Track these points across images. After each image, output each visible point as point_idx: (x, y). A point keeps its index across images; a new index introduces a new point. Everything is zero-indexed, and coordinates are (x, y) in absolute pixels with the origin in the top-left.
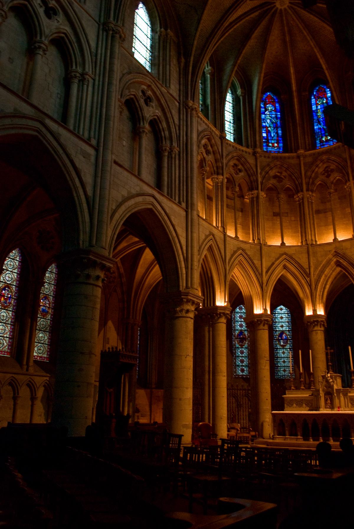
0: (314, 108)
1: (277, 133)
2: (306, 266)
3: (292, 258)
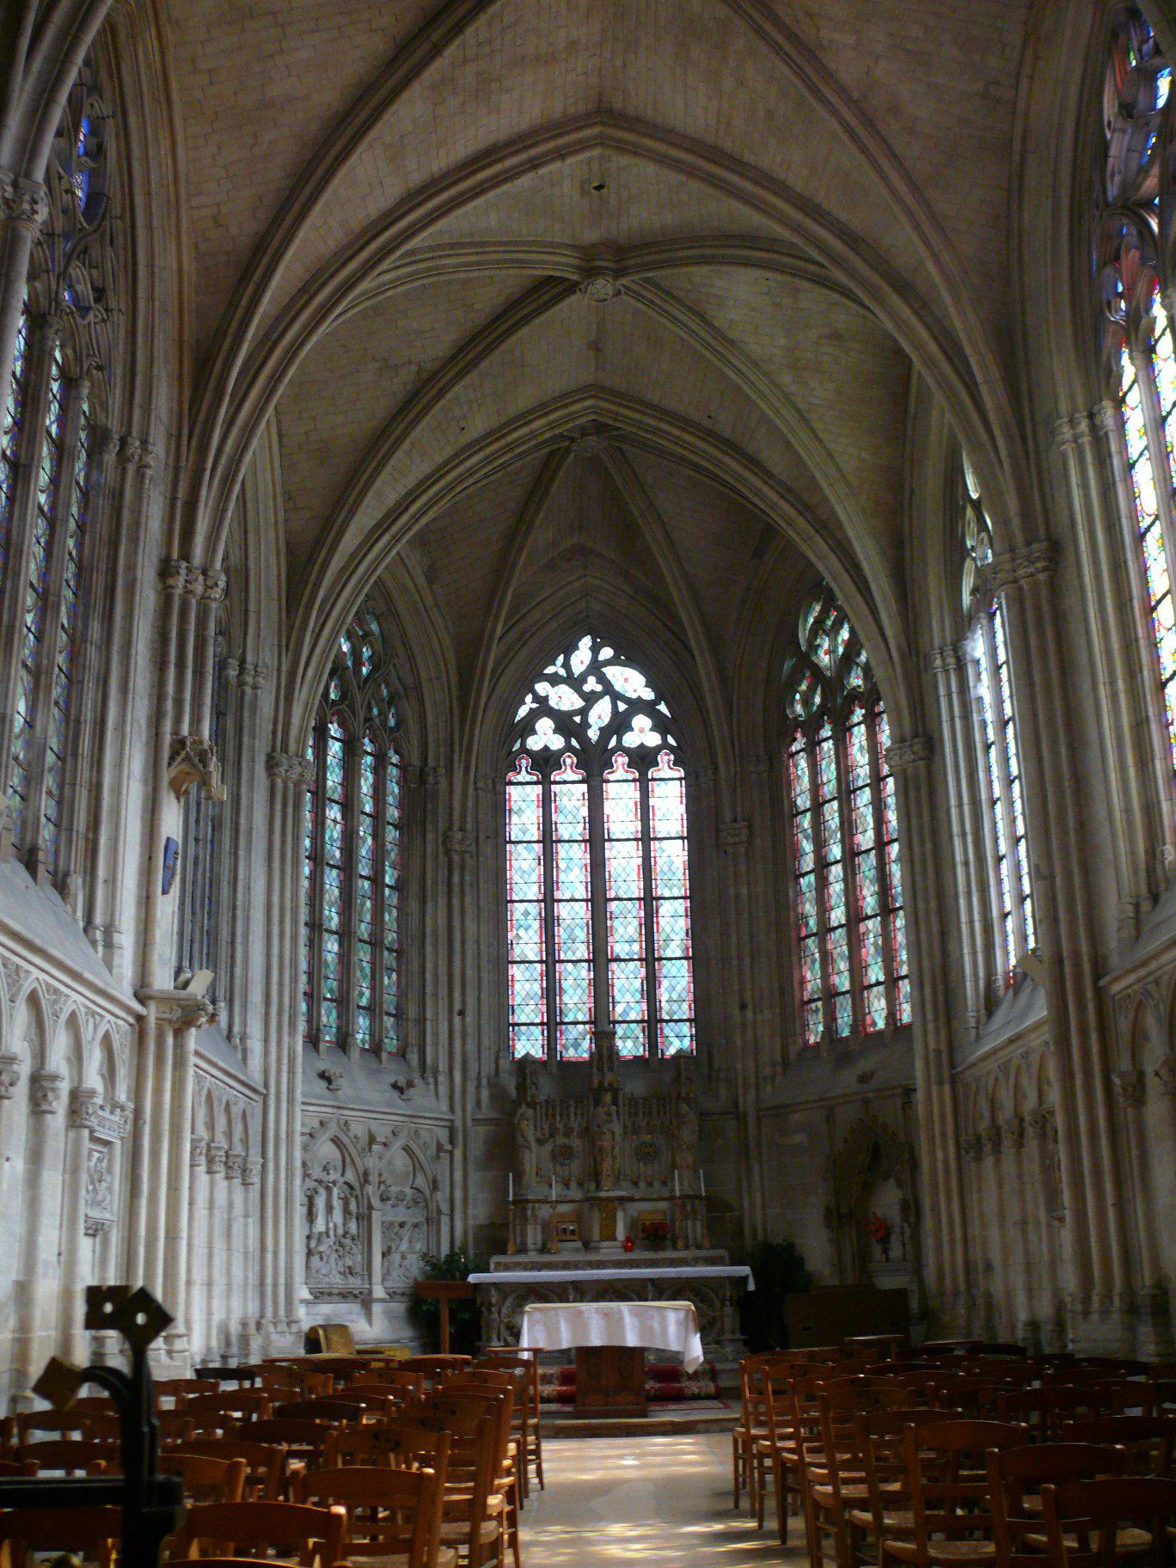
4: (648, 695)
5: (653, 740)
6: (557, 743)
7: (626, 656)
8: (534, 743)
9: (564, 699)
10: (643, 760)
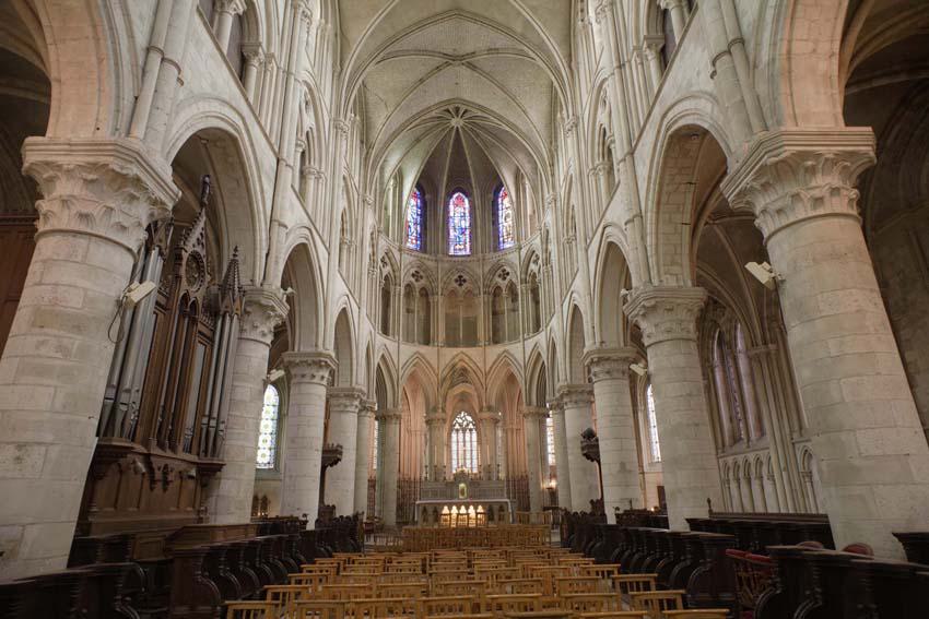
0: (451, 214)
9: (460, 421)
10: (471, 430)
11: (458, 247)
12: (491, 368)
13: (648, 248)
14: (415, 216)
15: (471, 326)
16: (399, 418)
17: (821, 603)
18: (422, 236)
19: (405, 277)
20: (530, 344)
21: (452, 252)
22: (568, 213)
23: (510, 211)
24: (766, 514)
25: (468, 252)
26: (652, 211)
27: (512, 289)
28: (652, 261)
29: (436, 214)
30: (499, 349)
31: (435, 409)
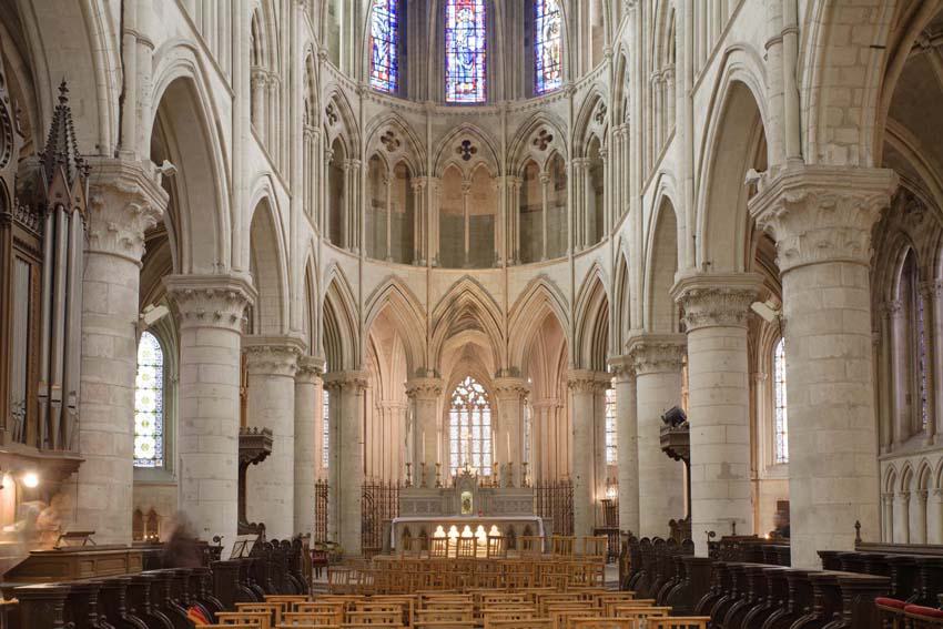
0: (451, 24)
1: (388, 52)
2: (423, 301)
3: (405, 287)
4: (483, 391)
5: (483, 402)
6: (461, 402)
7: (478, 382)
8: (456, 403)
9: (463, 392)
10: (481, 407)
11: (462, 87)
12: (517, 304)
13: (804, 94)
14: (385, 27)
15: (484, 230)
16: (362, 385)
17: (791, 611)
18: (399, 66)
19: (369, 144)
20: (583, 264)
21: (451, 98)
22: (662, 24)
23: (558, 20)
24: (926, 547)
25: (480, 97)
26: (635, 299)
27: (556, 163)
28: (808, 119)
29: (422, 23)
30: (529, 272)
31: (422, 373)
